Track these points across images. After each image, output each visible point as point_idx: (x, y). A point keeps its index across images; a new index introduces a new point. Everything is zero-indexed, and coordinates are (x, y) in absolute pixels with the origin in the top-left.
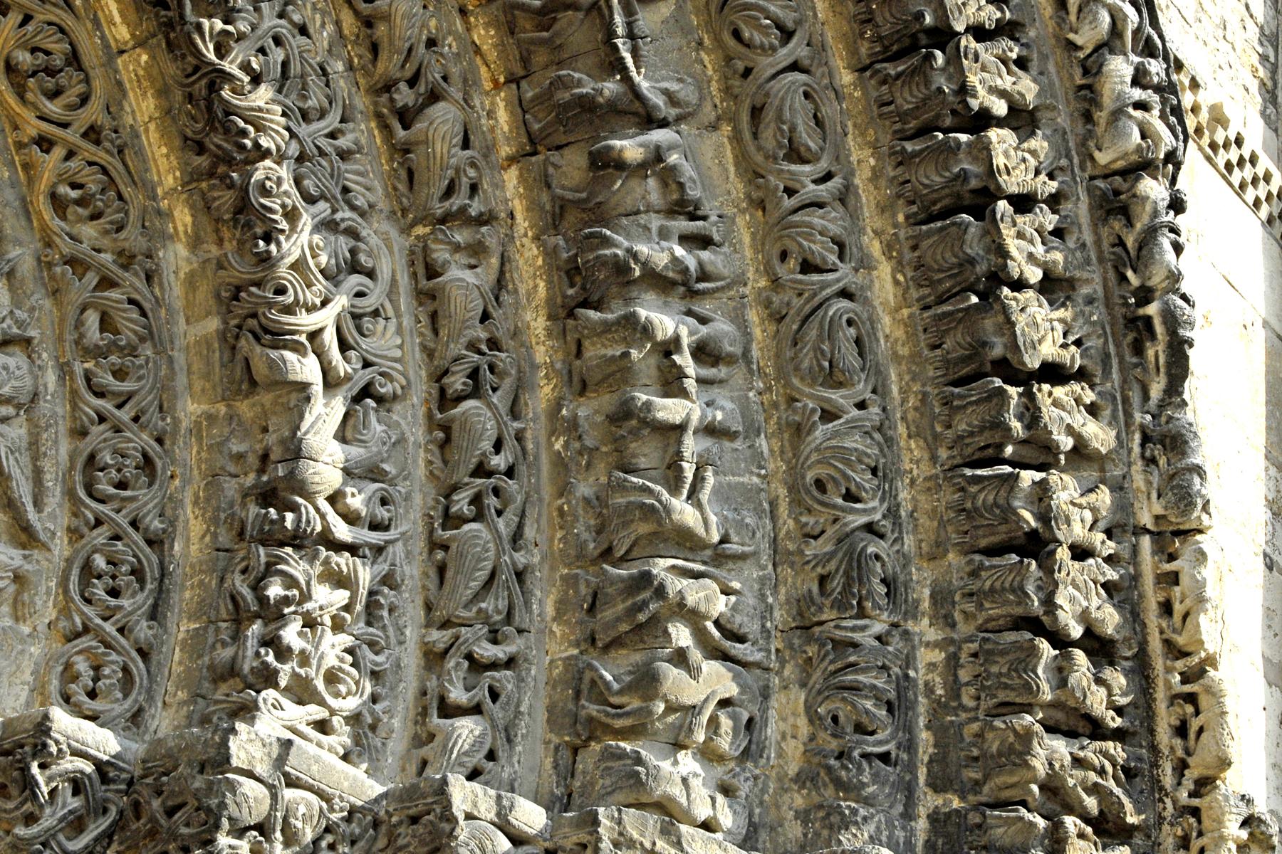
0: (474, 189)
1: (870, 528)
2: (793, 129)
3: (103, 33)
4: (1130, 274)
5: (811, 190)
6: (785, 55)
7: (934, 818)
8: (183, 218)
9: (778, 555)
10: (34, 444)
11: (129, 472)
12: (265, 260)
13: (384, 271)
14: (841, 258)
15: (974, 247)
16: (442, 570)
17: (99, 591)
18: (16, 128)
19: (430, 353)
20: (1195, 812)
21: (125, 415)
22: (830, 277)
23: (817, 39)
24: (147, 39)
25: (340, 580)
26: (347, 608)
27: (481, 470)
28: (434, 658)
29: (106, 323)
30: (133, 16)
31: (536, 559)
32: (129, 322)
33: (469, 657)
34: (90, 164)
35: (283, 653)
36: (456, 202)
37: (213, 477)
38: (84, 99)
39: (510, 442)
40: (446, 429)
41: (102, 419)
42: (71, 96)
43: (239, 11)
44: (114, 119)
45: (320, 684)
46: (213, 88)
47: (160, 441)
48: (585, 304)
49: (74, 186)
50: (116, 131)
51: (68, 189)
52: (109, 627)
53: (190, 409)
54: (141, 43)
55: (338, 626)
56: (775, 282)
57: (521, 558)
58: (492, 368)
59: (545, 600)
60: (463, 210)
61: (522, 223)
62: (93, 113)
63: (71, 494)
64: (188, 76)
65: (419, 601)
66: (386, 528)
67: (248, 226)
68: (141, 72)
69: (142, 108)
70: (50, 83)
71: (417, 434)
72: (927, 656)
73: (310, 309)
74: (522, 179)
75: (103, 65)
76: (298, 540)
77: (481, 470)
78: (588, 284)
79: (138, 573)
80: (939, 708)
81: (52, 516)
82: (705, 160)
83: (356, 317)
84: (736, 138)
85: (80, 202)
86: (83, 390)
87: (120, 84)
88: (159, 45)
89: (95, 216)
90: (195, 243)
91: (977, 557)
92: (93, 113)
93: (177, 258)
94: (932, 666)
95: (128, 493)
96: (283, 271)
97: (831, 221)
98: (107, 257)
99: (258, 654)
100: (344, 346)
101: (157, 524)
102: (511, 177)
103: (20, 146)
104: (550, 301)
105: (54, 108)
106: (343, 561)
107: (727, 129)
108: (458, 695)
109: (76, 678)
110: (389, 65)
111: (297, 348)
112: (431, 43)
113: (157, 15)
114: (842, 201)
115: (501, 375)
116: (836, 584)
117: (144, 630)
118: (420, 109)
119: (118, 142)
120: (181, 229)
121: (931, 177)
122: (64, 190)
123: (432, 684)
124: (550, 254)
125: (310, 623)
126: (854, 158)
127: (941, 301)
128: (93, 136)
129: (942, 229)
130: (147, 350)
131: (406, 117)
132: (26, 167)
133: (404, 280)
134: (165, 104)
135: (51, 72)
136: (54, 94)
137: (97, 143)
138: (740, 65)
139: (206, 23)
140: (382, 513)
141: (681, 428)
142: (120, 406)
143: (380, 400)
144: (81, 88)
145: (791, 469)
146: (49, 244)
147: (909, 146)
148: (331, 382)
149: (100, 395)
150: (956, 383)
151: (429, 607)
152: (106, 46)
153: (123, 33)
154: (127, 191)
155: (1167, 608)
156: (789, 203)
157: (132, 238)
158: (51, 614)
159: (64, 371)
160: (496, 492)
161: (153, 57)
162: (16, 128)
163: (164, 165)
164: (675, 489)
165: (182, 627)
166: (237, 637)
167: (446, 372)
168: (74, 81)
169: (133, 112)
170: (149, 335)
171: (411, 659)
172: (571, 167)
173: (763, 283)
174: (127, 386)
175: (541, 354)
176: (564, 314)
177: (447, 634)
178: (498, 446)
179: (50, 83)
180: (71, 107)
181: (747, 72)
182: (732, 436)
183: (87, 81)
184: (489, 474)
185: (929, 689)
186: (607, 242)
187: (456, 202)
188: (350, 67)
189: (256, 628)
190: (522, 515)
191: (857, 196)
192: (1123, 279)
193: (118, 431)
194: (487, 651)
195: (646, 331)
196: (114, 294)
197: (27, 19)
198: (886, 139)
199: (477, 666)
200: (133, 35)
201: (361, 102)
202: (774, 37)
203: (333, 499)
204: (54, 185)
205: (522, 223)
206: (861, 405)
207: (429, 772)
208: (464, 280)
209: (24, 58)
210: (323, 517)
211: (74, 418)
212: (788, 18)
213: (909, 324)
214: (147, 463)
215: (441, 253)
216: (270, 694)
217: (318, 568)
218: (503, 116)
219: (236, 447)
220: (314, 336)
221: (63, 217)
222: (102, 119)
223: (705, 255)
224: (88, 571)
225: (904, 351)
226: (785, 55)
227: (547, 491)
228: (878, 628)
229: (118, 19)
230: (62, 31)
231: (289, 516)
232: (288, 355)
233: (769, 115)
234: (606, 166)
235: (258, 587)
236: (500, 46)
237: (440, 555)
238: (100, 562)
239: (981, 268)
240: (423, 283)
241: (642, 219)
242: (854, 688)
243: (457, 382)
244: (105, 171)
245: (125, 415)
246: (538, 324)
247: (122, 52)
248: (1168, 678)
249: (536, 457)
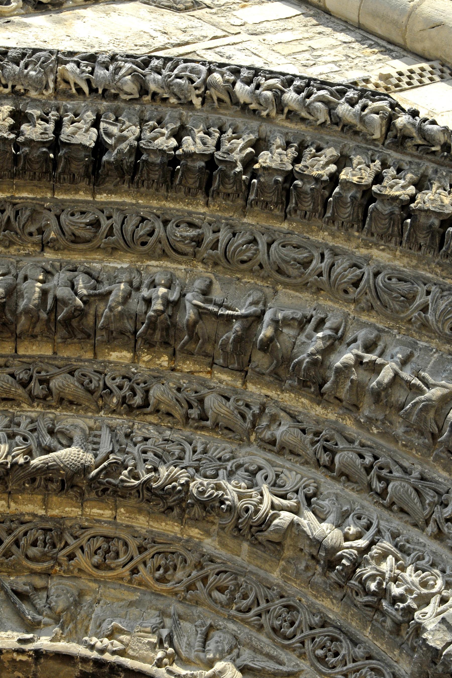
0: (247, 406)
2: (295, 260)
3: (103, 521)
4: (433, 149)
5: (324, 266)
6: (262, 246)
8: (195, 532)
10: (255, 650)
12: (231, 509)
13: (262, 462)
14: (360, 268)
15: (385, 209)
16: (402, 510)
17: (332, 660)
18: (122, 579)
19: (306, 463)
21: (263, 605)
22: (365, 277)
23: (263, 230)
24: (115, 504)
25: (383, 556)
26: (397, 560)
27: (368, 469)
29: (221, 590)
30: (104, 505)
31: (420, 468)
32: (225, 580)
34: (153, 557)
35: (402, 598)
36: (249, 416)
37: (310, 583)
38: (126, 544)
39: (362, 451)
40: (342, 474)
41: (260, 615)
42: (122, 549)
43: (124, 461)
44: (140, 537)
45: (424, 591)
46: (149, 489)
47: (282, 597)
48: (321, 386)
49: (158, 569)
50: (145, 539)
51: (159, 572)
52: (350, 665)
53: (275, 576)
54: (116, 508)
55: (403, 568)
56: (355, 301)
57: (415, 474)
58: (327, 440)
60: (254, 415)
61: (272, 394)
62: (133, 544)
63: (284, 647)
64: (139, 497)
65: (410, 528)
66: (371, 524)
67: (213, 508)
68: (127, 515)
69: (142, 523)
70: (112, 554)
71: (337, 487)
73: (261, 502)
74: (254, 384)
75: (116, 529)
77: (368, 469)
78: (313, 380)
79: (333, 639)
81: (290, 660)
82: (288, 303)
83: (274, 485)
84: (286, 285)
85: (166, 571)
87: (127, 526)
88: (120, 501)
89: (175, 568)
90: (208, 533)
92: (133, 544)
93: (210, 545)
95: (297, 623)
96: (239, 504)
97: (342, 264)
98: (194, 573)
99: (396, 610)
100: (284, 497)
101: (317, 619)
102: (251, 387)
103: (130, 581)
104: (311, 400)
105: (123, 559)
106: (375, 550)
107: (280, 287)
110: (178, 412)
111: (275, 517)
112: (179, 390)
113: (108, 495)
114: (336, 255)
115: (332, 438)
117: (359, 651)
118: (203, 410)
119: (150, 541)
120: (199, 536)
121: (346, 212)
124: (292, 389)
125: (395, 580)
126: (321, 240)
127: (401, 235)
128: (142, 550)
129: (371, 219)
130: (241, 579)
131: (203, 417)
132: (140, 584)
133: (270, 456)
134: (146, 512)
135: (108, 551)
136: (117, 555)
137: (146, 549)
138: (256, 267)
139: (122, 477)
140: (364, 522)
141: (396, 374)
142: (258, 605)
143: (315, 495)
144: (121, 543)
145: (439, 337)
146: (176, 594)
147: (328, 214)
148: (296, 511)
149: (249, 610)
150: (441, 247)
151: (415, 525)
152: (109, 523)
153: (108, 513)
154: (172, 549)
156: (325, 278)
157: (192, 558)
159: (231, 618)
160: (381, 468)
161: (124, 506)
162: (122, 579)
163: (169, 528)
164: (422, 392)
165: (366, 635)
166: (384, 614)
167: (318, 460)
168: (116, 544)
169: (141, 527)
170: (236, 575)
171: (435, 546)
172: (260, 360)
173: (353, 307)
175: (332, 417)
176: (320, 397)
177: (432, 524)
178: (362, 457)
179: (112, 554)
180: (126, 551)
181: (261, 266)
182: (411, 355)
183: (119, 539)
184: (372, 467)
186: (300, 363)
187: (249, 416)
188: (171, 428)
189: (385, 604)
190: (397, 463)
191: (338, 247)
192: (434, 152)
193: (268, 611)
195: (346, 367)
196: (211, 579)
197: (82, 548)
198: (320, 223)
200: (111, 509)
201: (187, 432)
202: (253, 247)
203: (346, 539)
204: (154, 577)
205: (272, 394)
206: (428, 293)
208: (283, 431)
209: (97, 559)
210: (352, 547)
211: (253, 627)
212: (248, 237)
213: (404, 254)
214: (288, 607)
215: (267, 435)
216: (417, 614)
217: (373, 562)
218: (224, 377)
219: (302, 566)
220: (273, 506)
221: (169, 581)
222: (138, 542)
223: (328, 324)
224: (321, 660)
225: (414, 262)
226: (262, 246)
227: (392, 446)
229: (101, 512)
230: (94, 537)
231: (344, 561)
232: (276, 522)
233: (283, 266)
234: (268, 346)
235: (367, 592)
236: (196, 362)
237: (395, 508)
238: (320, 652)
239: (397, 211)
240: (275, 449)
241: (298, 343)
243: (325, 458)
244: (159, 553)
245: (263, 605)
246: (318, 411)
247: (115, 517)
249: (375, 443)
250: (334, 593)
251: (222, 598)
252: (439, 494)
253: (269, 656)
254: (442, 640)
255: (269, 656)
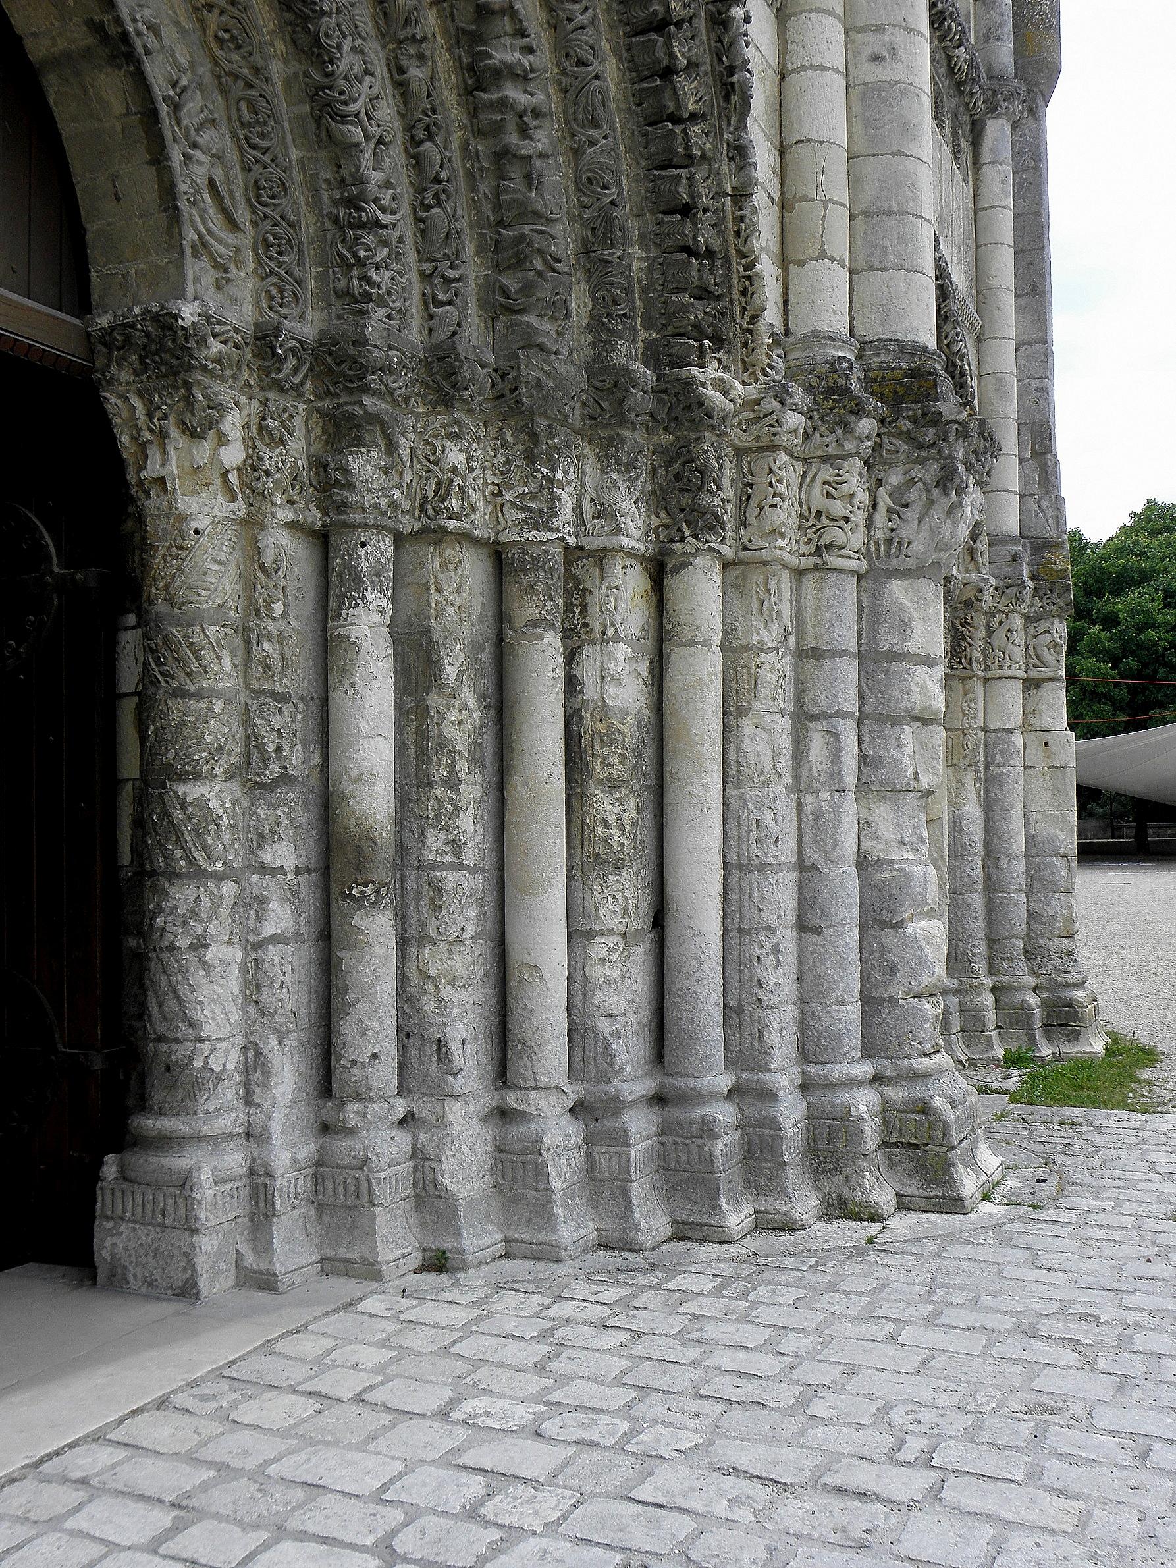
1: (612, 203)
4: (724, 58)
7: (645, 341)
9: (572, 218)
10: (227, 175)
11: (276, 191)
13: (378, 74)
15: (660, 53)
16: (423, 231)
20: (750, 331)
22: (590, 68)
27: (437, 180)
28: (426, 277)
29: (253, 109)
33: (443, 277)
34: (233, 18)
41: (257, 161)
49: (225, 31)
56: (563, 72)
59: (469, 248)
63: (249, 202)
71: (402, 160)
72: (637, 265)
76: (362, 226)
78: (478, 78)
79: (289, 241)
80: (644, 291)
86: (246, 147)
89: (238, 47)
91: (661, 216)
94: (640, 270)
95: (276, 201)
99: (361, 286)
100: (369, 118)
108: (441, 296)
109: (272, 298)
111: (352, 123)
115: (439, 128)
116: (601, 232)
120: (279, 52)
122: (221, 34)
123: (428, 291)
127: (643, 80)
129: (644, 42)
133: (387, 76)
142: (263, 154)
145: (575, 172)
146: (216, 64)
148: (368, 138)
149: (254, 148)
150: (649, 125)
155: (738, 234)
158: (252, 266)
159: (234, 134)
167: (414, 126)
170: (273, 116)
171: (415, 278)
174: (265, 143)
182: (547, 156)
184: (440, 182)
185: (640, 281)
192: (720, 60)
193: (265, 168)
194: (452, 274)
199: (447, 281)
206: (605, 137)
207: (435, 334)
211: (243, 162)
213: (625, 92)
215: (405, 62)
221: (222, 49)
223: (531, 57)
225: (623, 106)
228: (619, 253)
237: (422, 226)
239: (663, 65)
240: (396, 77)
242: (611, 284)
245: (267, 159)
248: (737, 268)
250: (326, 220)
251: (246, 116)
252: (457, 258)
253: (231, 192)
254: (375, 339)
255: (231, 192)
